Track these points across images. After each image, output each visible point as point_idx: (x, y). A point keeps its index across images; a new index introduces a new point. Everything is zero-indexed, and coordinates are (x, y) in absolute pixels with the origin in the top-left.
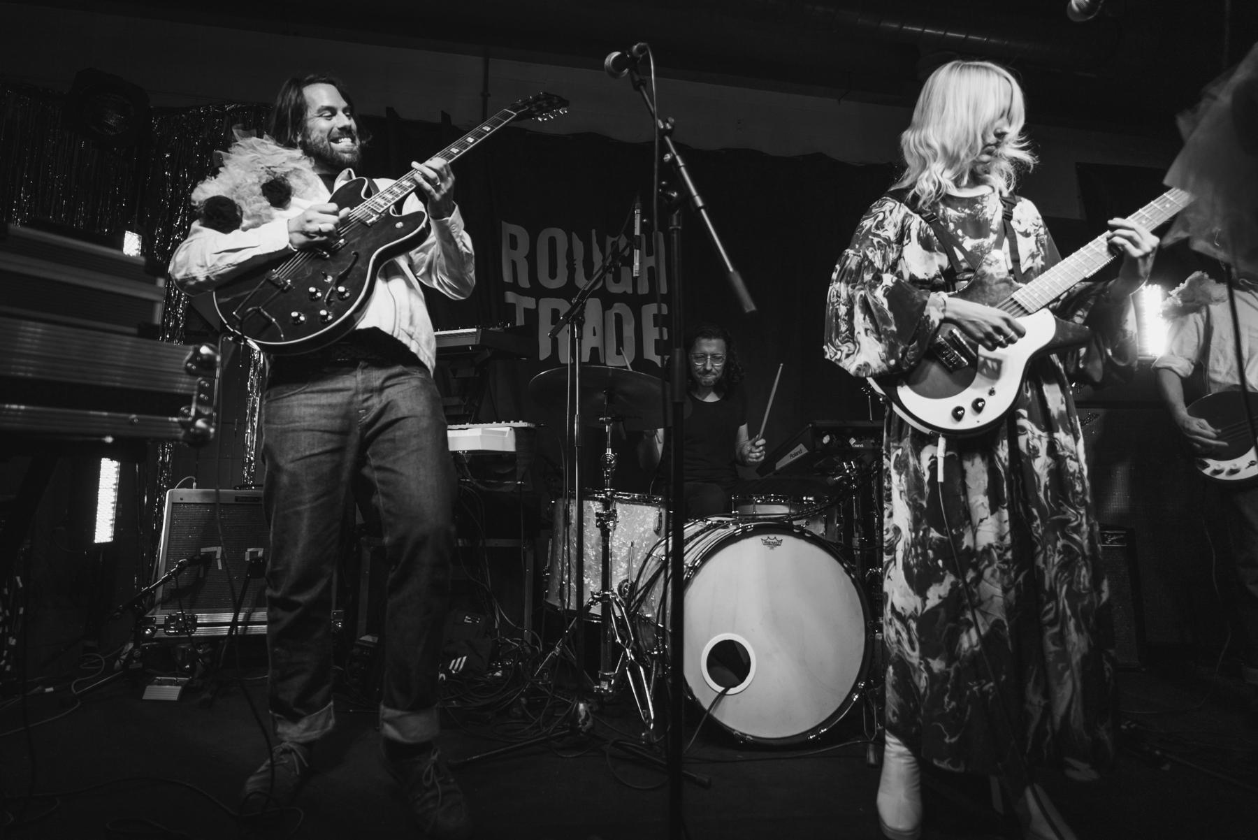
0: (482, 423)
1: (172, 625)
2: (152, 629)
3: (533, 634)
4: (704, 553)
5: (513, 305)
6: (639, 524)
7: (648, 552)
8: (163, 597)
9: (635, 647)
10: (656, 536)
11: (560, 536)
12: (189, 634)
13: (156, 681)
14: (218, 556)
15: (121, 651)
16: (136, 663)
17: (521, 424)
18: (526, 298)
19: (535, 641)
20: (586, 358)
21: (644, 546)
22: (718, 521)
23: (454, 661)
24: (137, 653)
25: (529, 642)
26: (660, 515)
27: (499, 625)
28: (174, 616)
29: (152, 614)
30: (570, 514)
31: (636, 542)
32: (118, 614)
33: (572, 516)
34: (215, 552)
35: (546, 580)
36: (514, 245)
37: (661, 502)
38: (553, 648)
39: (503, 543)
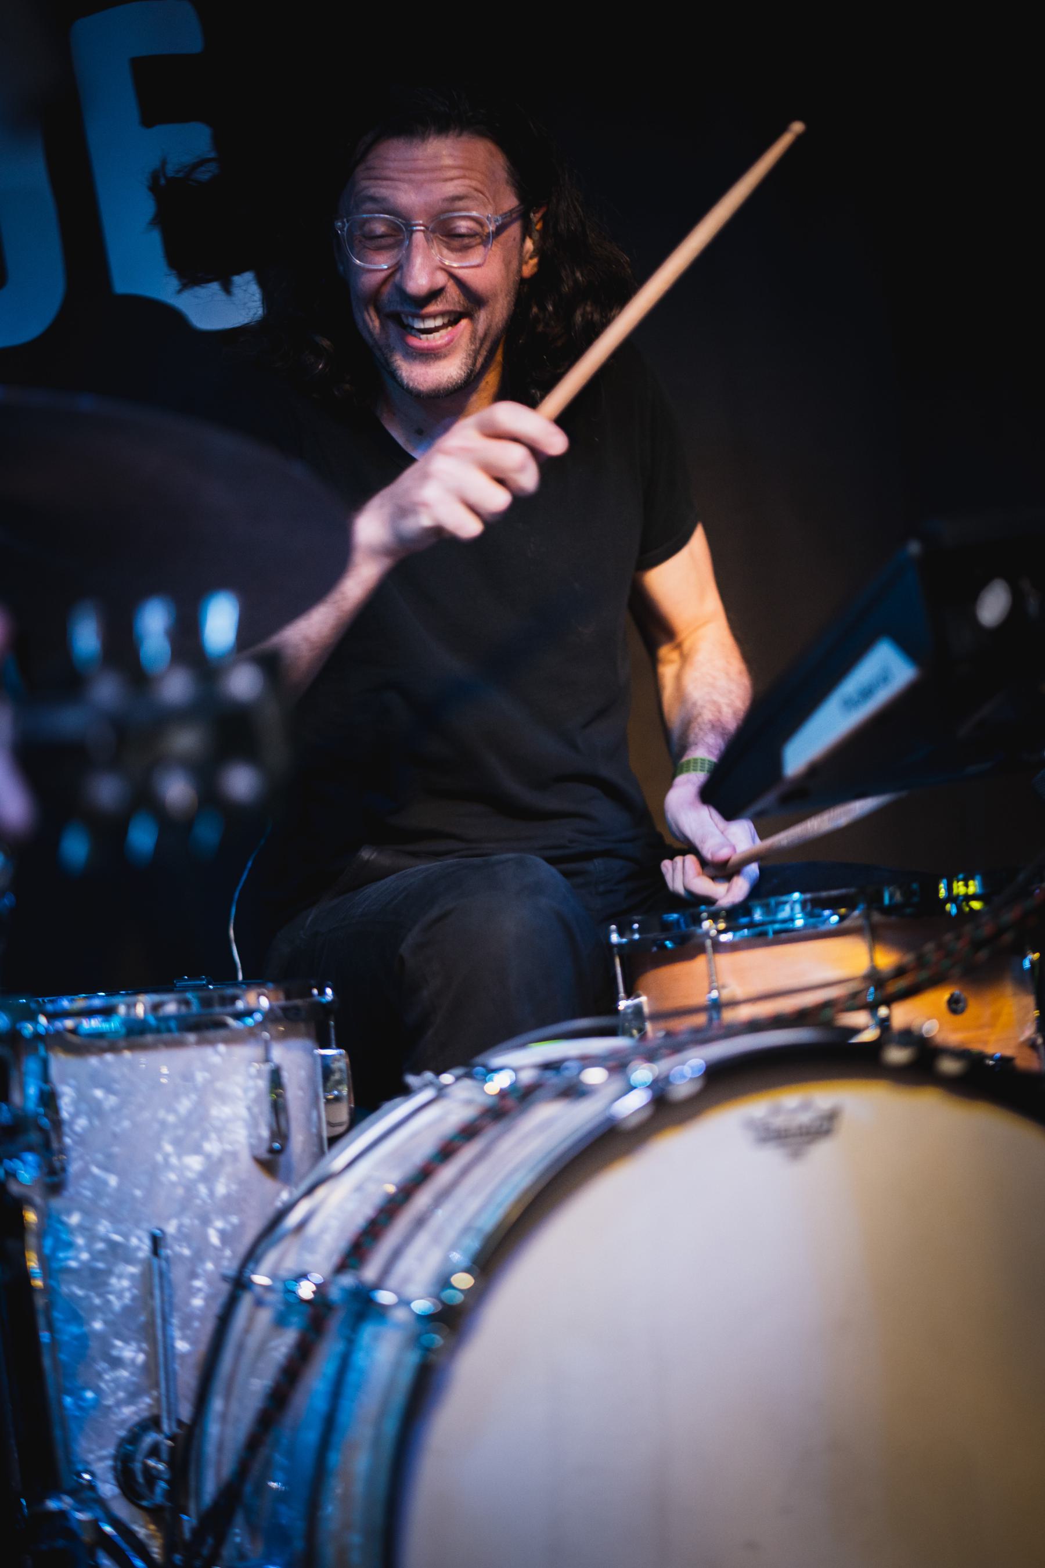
6: (177, 1142)
10: (269, 1184)
21: (214, 1239)
26: (276, 1079)
31: (171, 1228)
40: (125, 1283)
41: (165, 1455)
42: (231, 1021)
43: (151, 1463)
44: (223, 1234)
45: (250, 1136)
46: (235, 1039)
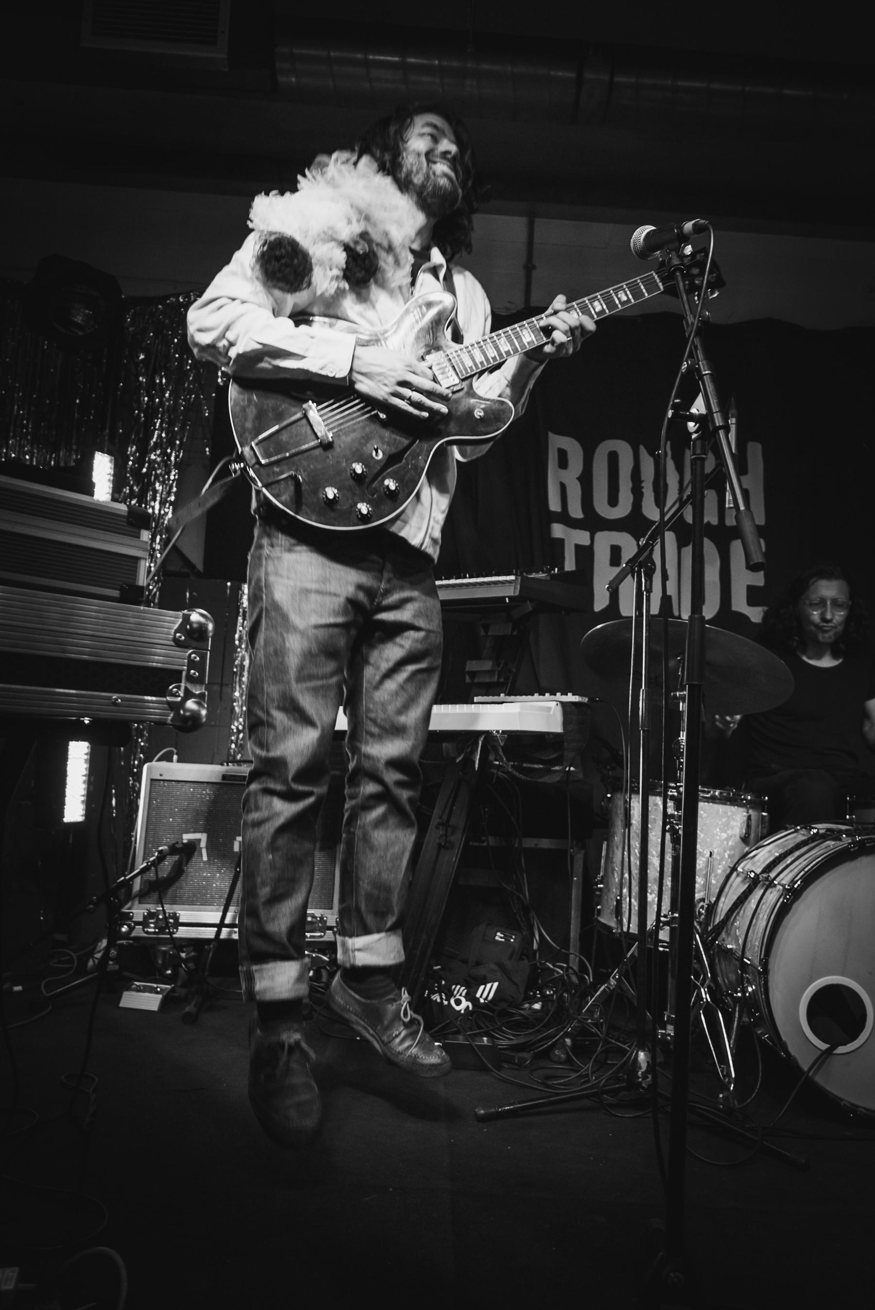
0: (521, 695)
1: (151, 923)
2: (129, 926)
3: (580, 960)
4: (806, 872)
5: (562, 541)
6: (720, 829)
7: (732, 866)
8: (141, 890)
9: (712, 984)
10: (743, 845)
11: (617, 839)
12: (171, 934)
13: (134, 986)
14: (203, 844)
15: (95, 948)
16: (113, 964)
17: (571, 698)
18: (578, 531)
19: (583, 969)
20: (655, 610)
21: (727, 856)
22: (828, 830)
23: (482, 987)
24: (113, 953)
25: (575, 968)
26: (749, 818)
27: (539, 945)
28: (154, 913)
29: (129, 909)
30: (631, 812)
31: (716, 851)
32: (91, 906)
33: (633, 814)
34: (199, 840)
35: (598, 893)
36: (563, 463)
37: (749, 802)
38: (605, 979)
39: (545, 844)
40: (701, 862)
41: (705, 909)
42: (739, 800)
43: (701, 910)
44: (729, 855)
45: (740, 831)
46: (740, 806)
